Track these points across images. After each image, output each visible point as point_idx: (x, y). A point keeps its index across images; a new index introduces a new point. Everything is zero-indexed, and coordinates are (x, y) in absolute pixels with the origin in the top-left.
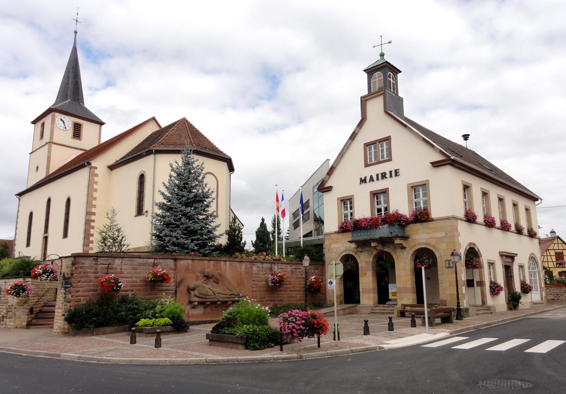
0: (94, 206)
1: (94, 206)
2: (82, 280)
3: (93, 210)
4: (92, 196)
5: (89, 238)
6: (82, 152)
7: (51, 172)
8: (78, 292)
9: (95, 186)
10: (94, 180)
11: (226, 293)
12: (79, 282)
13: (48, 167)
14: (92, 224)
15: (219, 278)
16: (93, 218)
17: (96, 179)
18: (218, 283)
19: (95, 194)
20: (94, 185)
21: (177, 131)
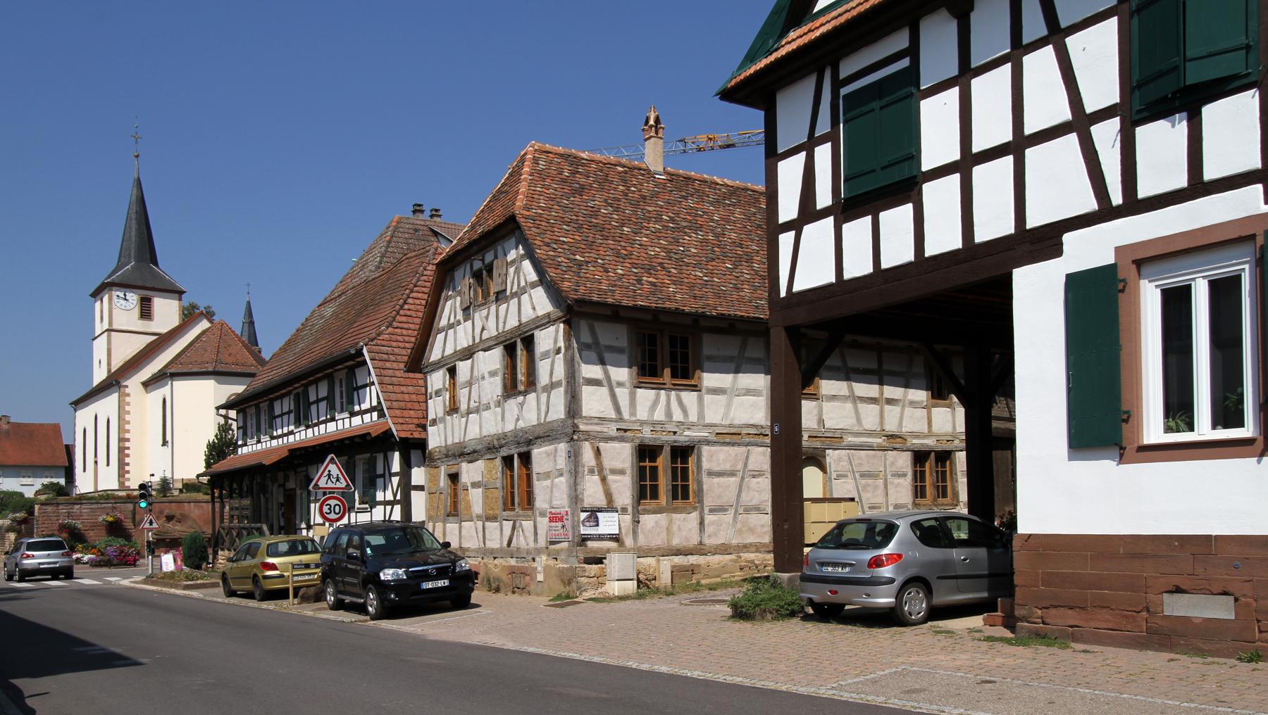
0: (128, 431)
1: (128, 431)
2: (46, 522)
3: (127, 436)
4: (124, 419)
5: (124, 468)
6: (154, 338)
7: (113, 371)
8: (43, 531)
9: (127, 408)
10: (125, 400)
11: (188, 530)
12: (44, 523)
13: (109, 364)
14: (127, 452)
15: (179, 517)
16: (127, 444)
17: (127, 399)
18: (180, 522)
19: (127, 418)
20: (126, 407)
21: (205, 342)
